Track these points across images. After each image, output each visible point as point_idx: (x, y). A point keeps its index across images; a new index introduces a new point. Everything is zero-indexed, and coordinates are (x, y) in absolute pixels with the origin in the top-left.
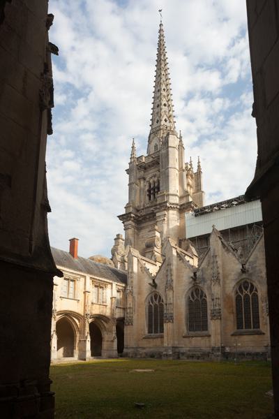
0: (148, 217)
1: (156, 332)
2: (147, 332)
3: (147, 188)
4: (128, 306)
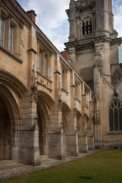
0: (86, 46)
1: (117, 129)
2: (109, 130)
3: (82, 26)
4: (97, 110)
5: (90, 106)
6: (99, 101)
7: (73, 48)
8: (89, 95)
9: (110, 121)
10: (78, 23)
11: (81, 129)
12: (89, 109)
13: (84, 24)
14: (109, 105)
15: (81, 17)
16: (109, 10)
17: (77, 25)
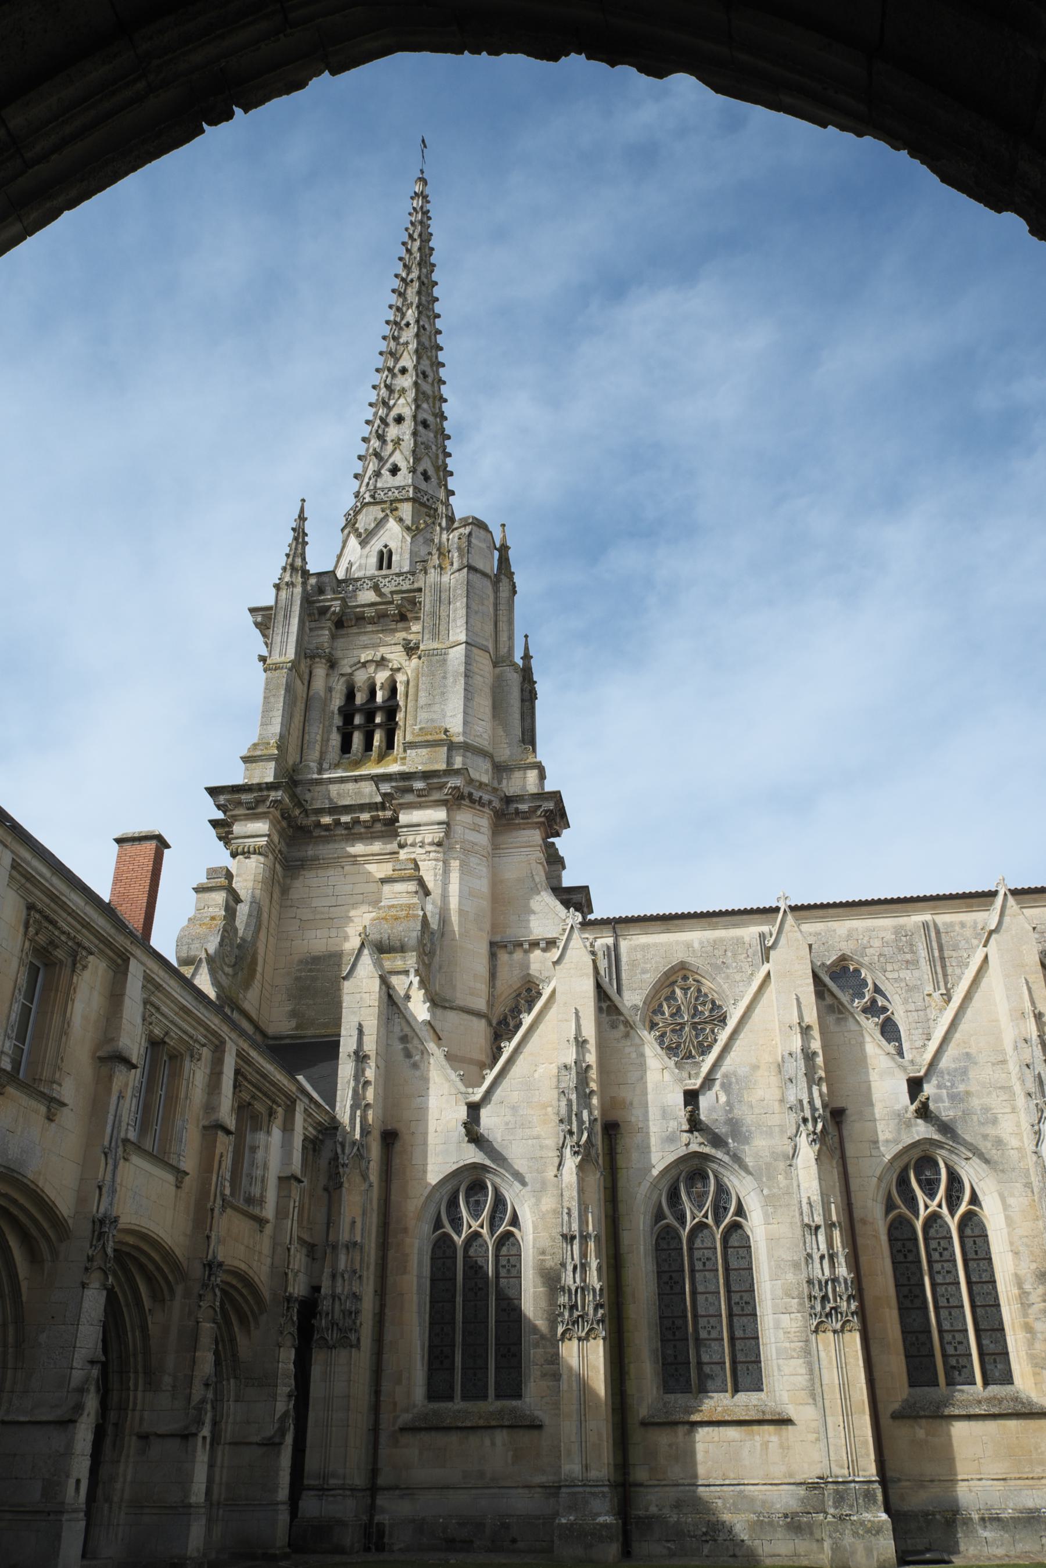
1: (475, 1392)
2: (419, 1392)
3: (337, 701)
4: (345, 1236)
5: (281, 1213)
6: (357, 1179)
7: (261, 827)
8: (288, 1128)
9: (432, 1324)
10: (319, 683)
11: (167, 1379)
12: (269, 1229)
13: (350, 695)
14: (432, 1210)
15: (338, 654)
16: (496, 641)
17: (311, 693)
